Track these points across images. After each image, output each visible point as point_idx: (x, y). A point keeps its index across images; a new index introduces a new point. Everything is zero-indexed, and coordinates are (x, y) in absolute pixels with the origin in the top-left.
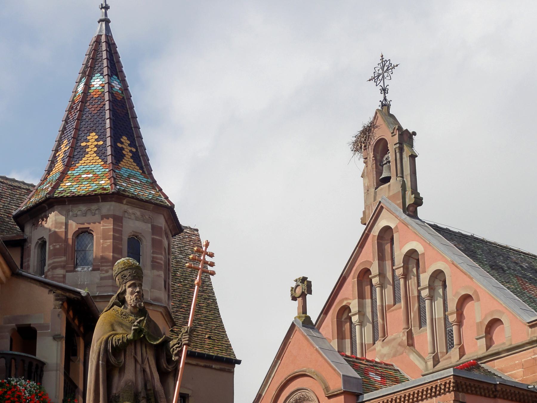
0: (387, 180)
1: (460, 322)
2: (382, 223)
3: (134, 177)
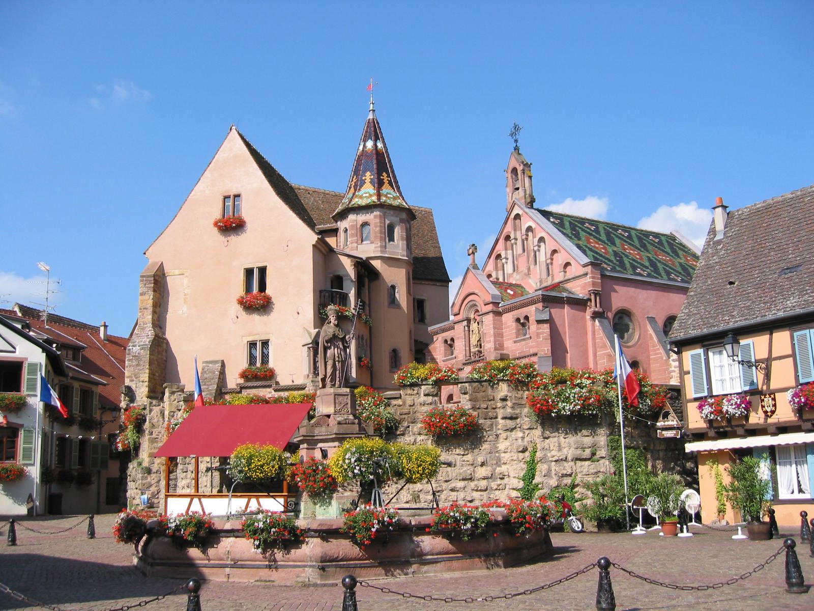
0: (518, 189)
1: (552, 264)
2: (515, 212)
3: (390, 194)
